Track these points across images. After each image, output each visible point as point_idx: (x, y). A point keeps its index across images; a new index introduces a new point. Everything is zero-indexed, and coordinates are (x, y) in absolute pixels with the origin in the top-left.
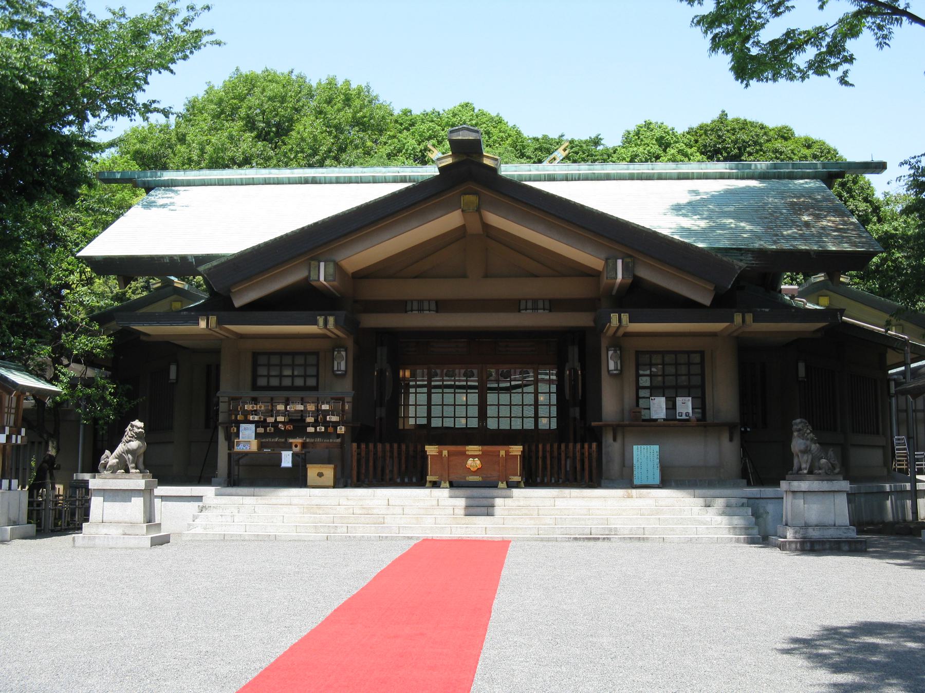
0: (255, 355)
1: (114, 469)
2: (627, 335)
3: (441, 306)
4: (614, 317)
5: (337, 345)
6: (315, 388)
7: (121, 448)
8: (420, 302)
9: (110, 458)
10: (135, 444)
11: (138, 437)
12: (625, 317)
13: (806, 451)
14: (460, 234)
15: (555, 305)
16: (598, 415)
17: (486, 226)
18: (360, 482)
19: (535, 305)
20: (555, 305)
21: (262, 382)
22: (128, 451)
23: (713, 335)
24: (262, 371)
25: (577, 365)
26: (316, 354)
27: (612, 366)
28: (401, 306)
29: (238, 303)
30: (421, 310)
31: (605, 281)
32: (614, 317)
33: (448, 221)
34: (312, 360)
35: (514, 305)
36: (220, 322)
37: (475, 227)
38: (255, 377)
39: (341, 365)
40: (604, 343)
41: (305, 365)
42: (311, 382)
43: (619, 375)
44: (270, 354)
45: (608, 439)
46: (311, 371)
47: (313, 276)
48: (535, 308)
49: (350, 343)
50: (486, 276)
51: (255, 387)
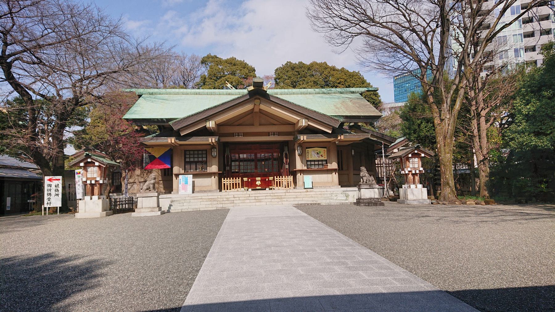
0: (185, 151)
5: (212, 146)
8: (238, 133)
14: (252, 111)
21: (188, 160)
23: (329, 142)
24: (188, 156)
26: (206, 150)
30: (238, 136)
33: (248, 107)
35: (268, 134)
37: (256, 110)
39: (215, 153)
41: (202, 154)
42: (204, 159)
46: (204, 156)
48: (274, 135)
50: (260, 125)
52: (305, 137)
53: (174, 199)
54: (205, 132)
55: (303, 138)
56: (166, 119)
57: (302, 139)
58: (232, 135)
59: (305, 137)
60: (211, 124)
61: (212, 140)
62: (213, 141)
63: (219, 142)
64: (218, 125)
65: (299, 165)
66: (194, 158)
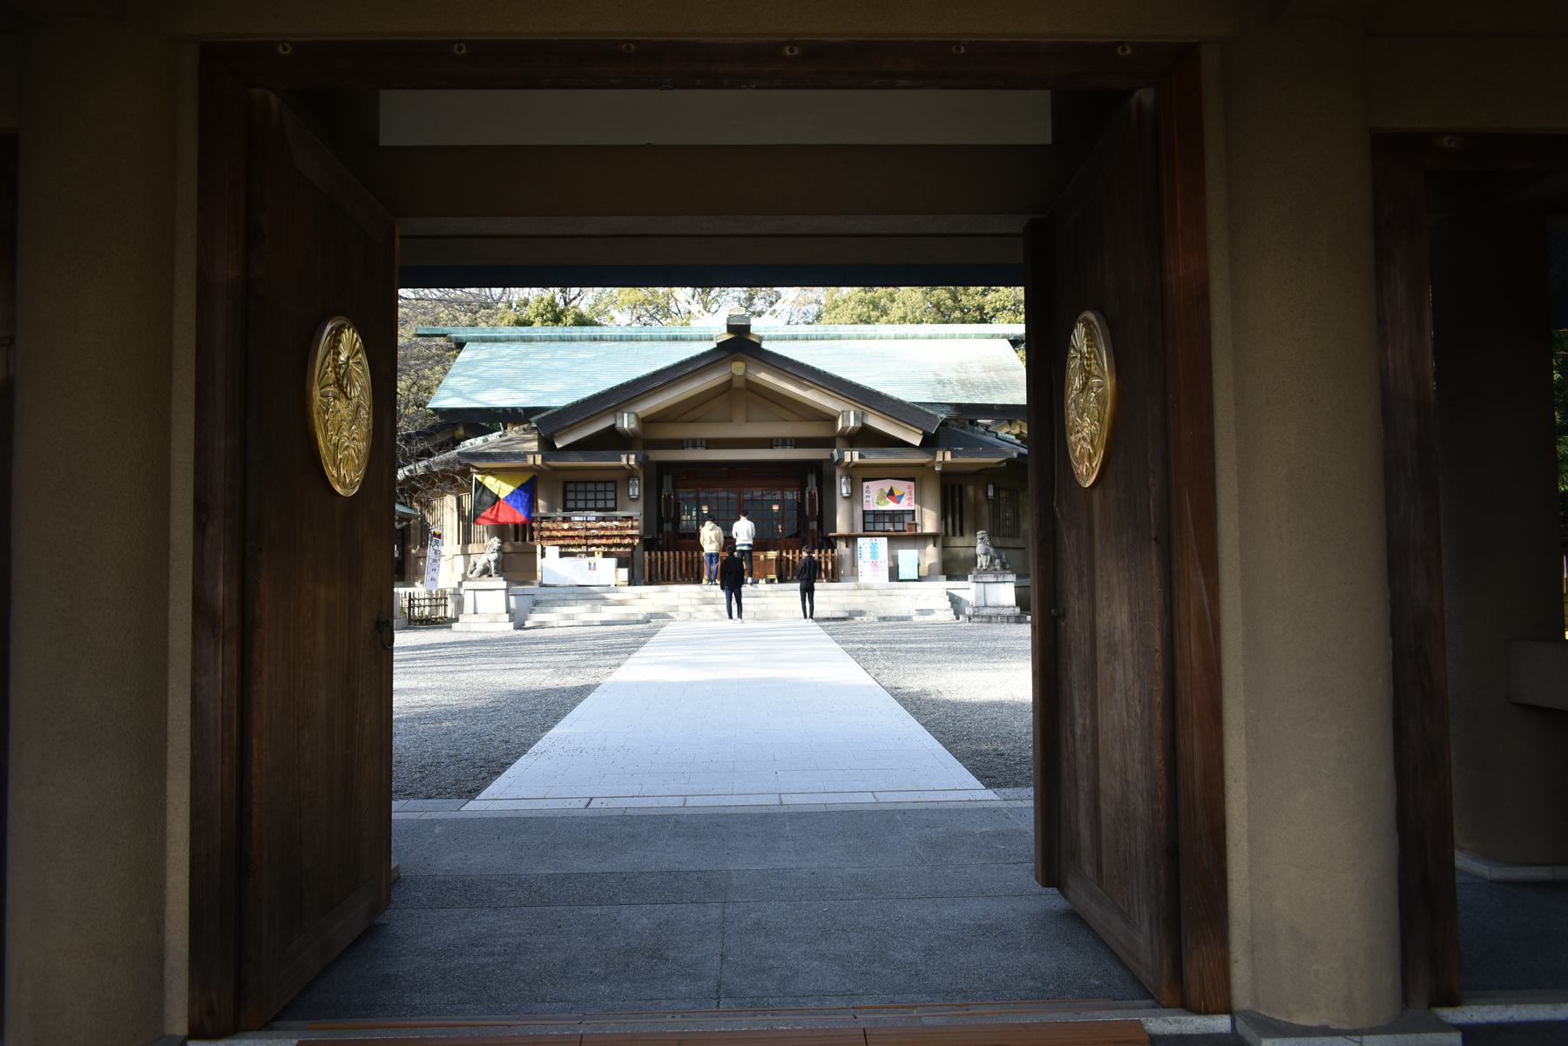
0: (566, 483)
2: (857, 466)
5: (629, 473)
6: (615, 509)
17: (748, 382)
18: (651, 581)
20: (799, 443)
24: (571, 496)
25: (815, 491)
26: (615, 482)
29: (559, 445)
34: (611, 487)
35: (768, 443)
38: (565, 501)
39: (635, 491)
42: (611, 504)
44: (576, 482)
46: (611, 495)
47: (619, 425)
49: (641, 474)
51: (565, 509)
53: (539, 598)
54: (613, 440)
55: (852, 456)
56: (525, 409)
57: (847, 459)
58: (680, 444)
59: (856, 454)
60: (627, 422)
61: (629, 460)
62: (632, 463)
63: (643, 463)
64: (646, 421)
65: (842, 527)
66: (586, 500)
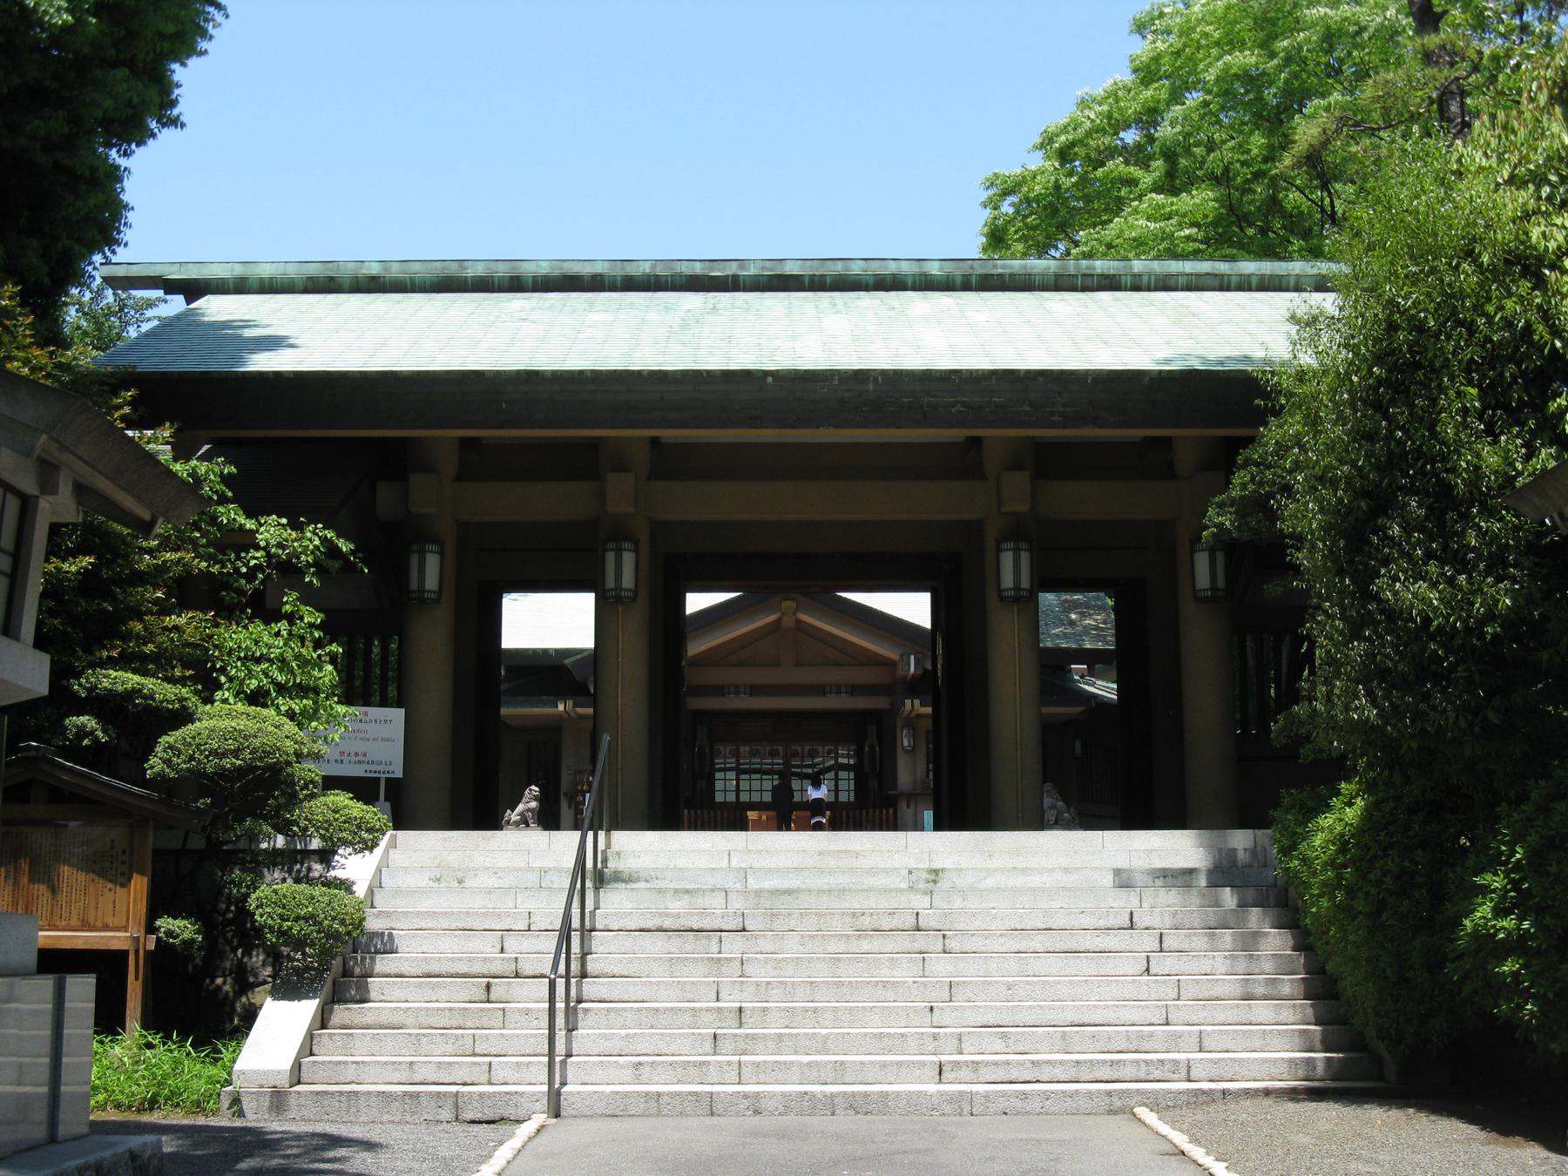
1: (517, 824)
3: (755, 690)
4: (908, 702)
7: (520, 807)
8: (737, 687)
9: (514, 816)
10: (533, 804)
11: (536, 798)
12: (917, 702)
13: (1052, 807)
14: (775, 627)
15: (855, 690)
16: (894, 786)
17: (798, 621)
19: (838, 689)
20: (855, 690)
22: (529, 810)
27: (906, 743)
28: (720, 690)
30: (737, 693)
31: (900, 672)
32: (908, 702)
35: (820, 690)
36: (575, 706)
37: (788, 622)
40: (899, 724)
43: (912, 751)
45: (903, 806)
48: (838, 692)
50: (797, 665)
52: (917, 702)
56: (558, 651)
58: (720, 690)
